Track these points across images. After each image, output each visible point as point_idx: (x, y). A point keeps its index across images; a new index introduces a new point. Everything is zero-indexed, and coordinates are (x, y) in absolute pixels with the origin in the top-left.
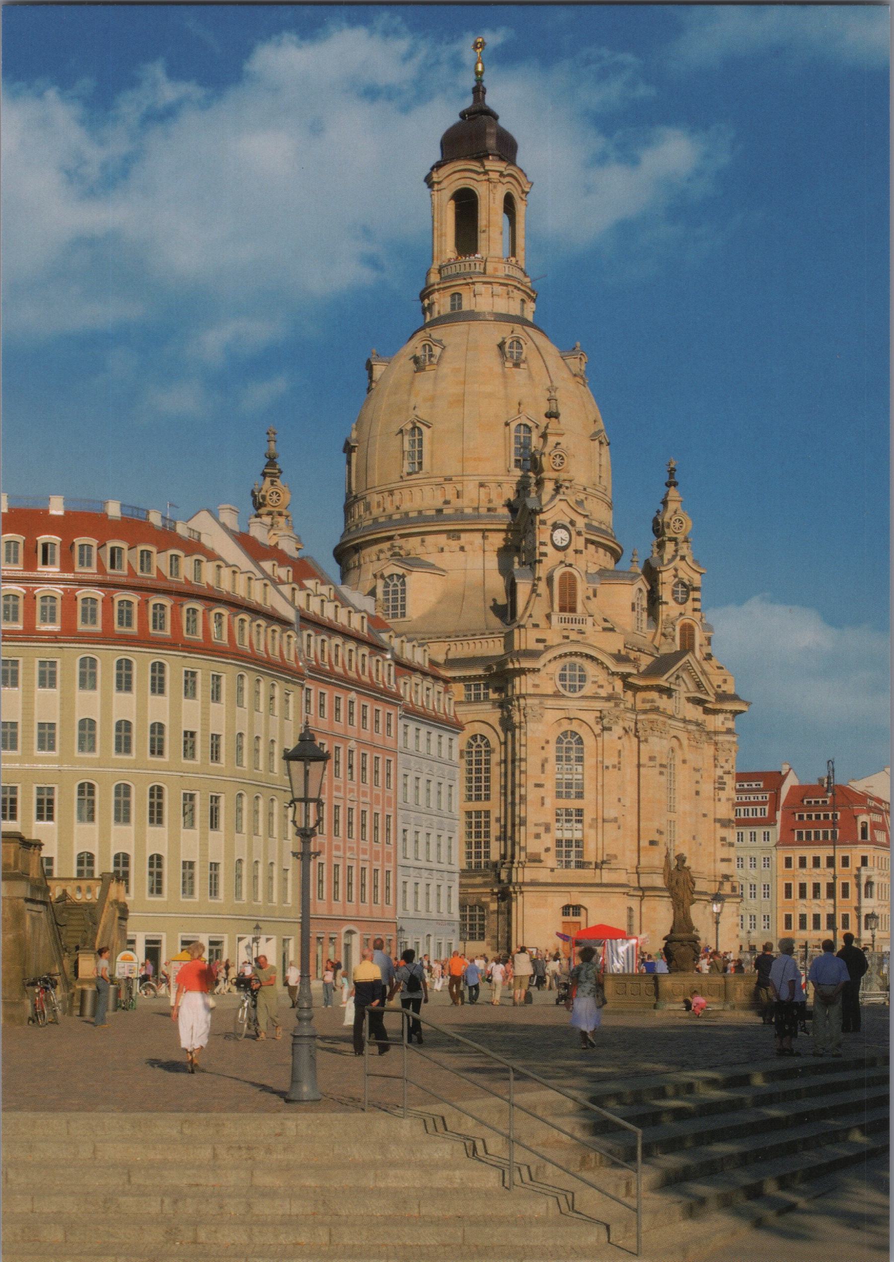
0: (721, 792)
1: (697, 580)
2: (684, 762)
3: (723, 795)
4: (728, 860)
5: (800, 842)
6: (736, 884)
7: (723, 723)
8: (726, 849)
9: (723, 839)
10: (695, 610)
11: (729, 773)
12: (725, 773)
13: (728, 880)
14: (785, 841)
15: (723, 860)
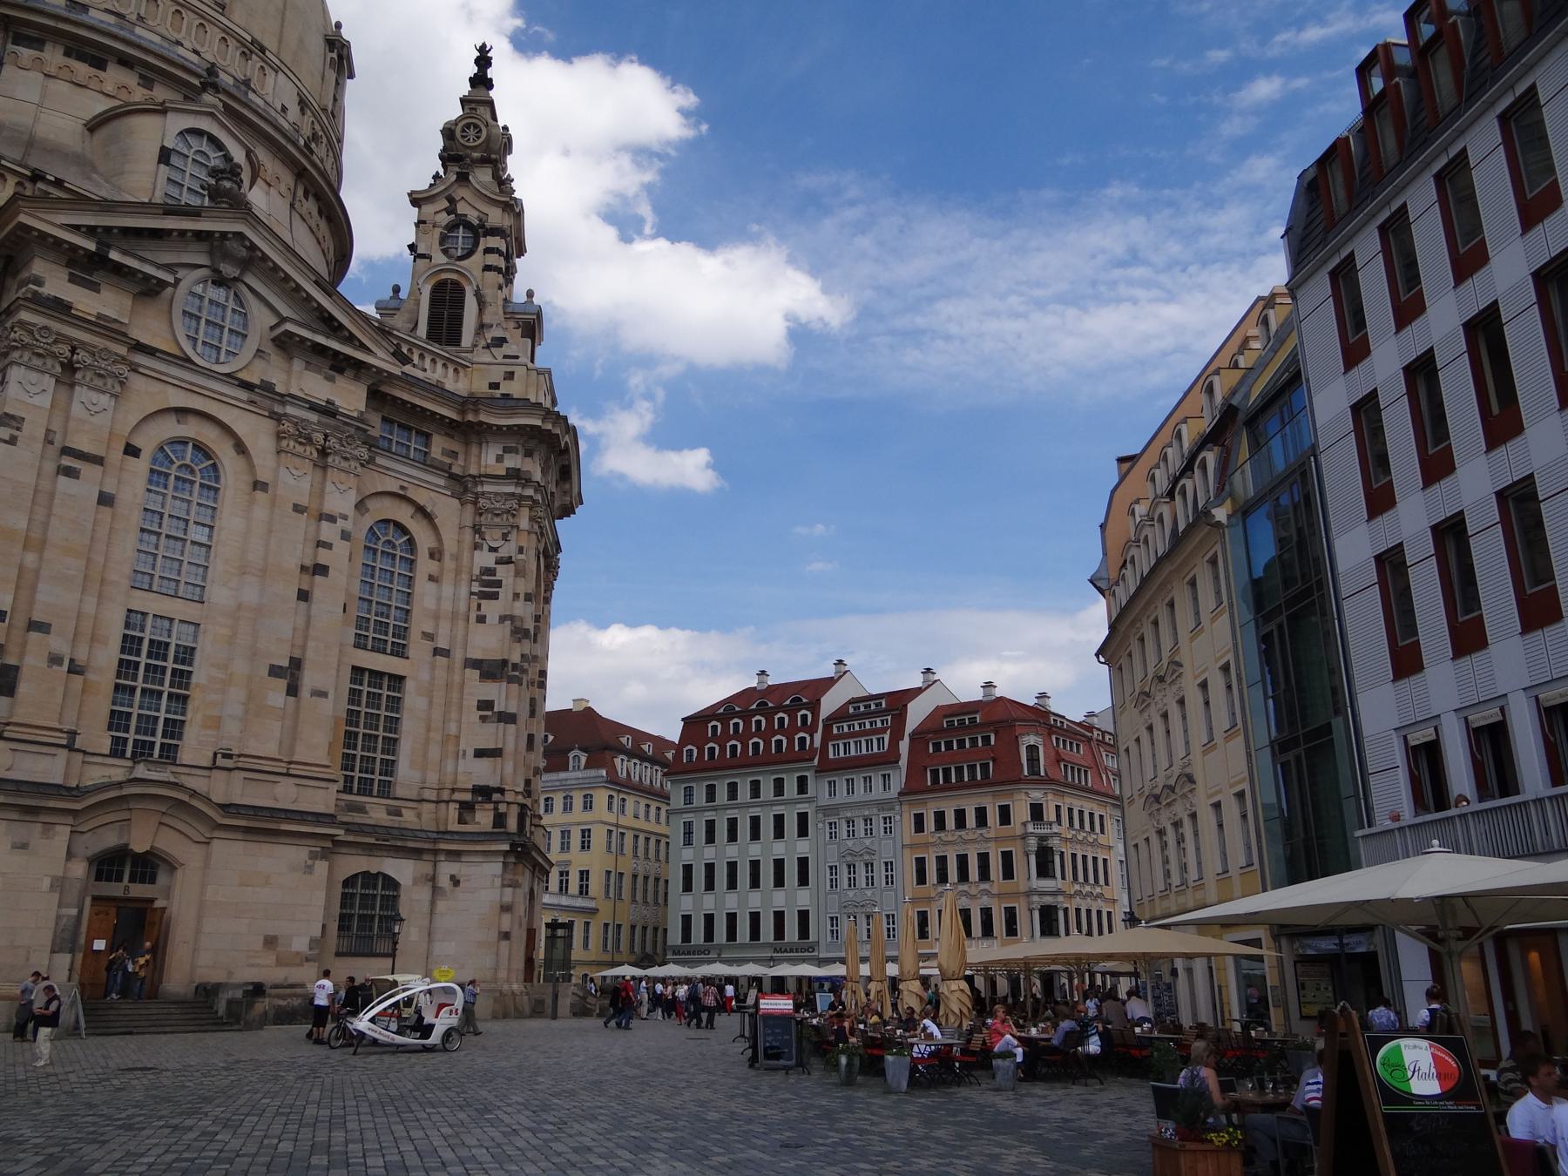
0: (483, 602)
1: (496, 217)
2: (259, 486)
3: (492, 609)
4: (495, 753)
5: (935, 788)
6: (502, 808)
7: (499, 459)
8: (491, 727)
9: (485, 705)
10: (487, 268)
11: (509, 561)
12: (499, 562)
13: (489, 800)
14: (911, 790)
15: (480, 753)
